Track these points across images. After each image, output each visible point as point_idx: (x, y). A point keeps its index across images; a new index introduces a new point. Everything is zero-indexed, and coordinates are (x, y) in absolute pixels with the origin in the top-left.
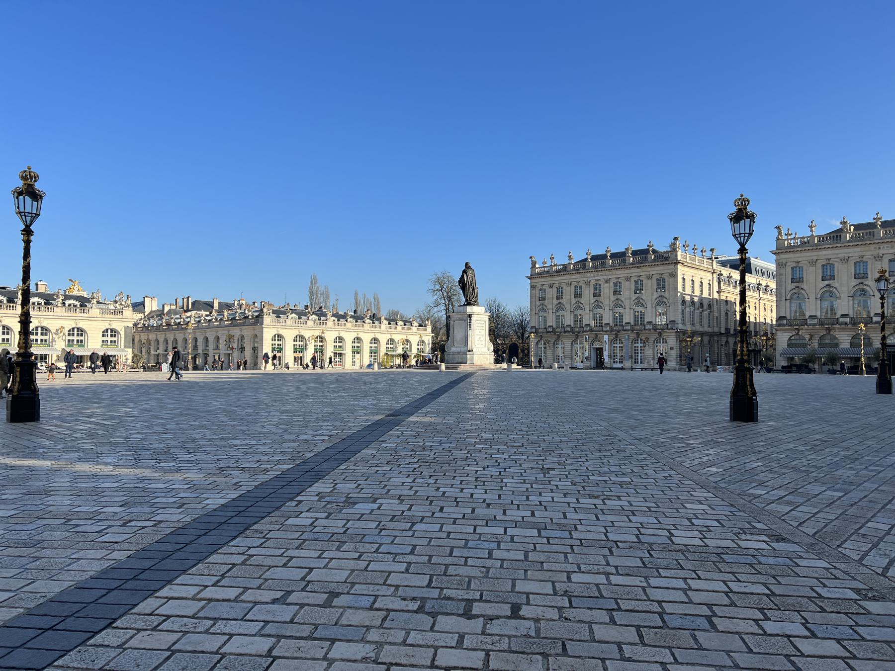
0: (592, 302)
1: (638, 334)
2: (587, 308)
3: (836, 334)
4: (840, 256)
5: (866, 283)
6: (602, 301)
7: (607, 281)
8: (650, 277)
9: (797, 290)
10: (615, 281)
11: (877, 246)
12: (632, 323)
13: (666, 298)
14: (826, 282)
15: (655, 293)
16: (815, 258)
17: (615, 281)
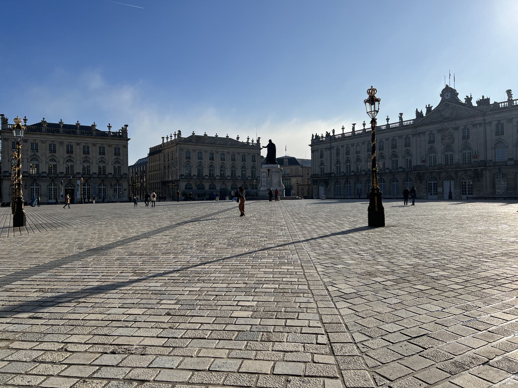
0: (66, 156)
1: (103, 181)
2: (61, 161)
3: (204, 183)
4: (205, 149)
5: (213, 162)
6: (74, 157)
7: (78, 144)
8: (110, 146)
9: (188, 163)
10: (100, 146)
11: (217, 147)
12: (47, 172)
13: (121, 160)
14: (200, 160)
15: (114, 156)
16: (195, 149)
17: (50, 143)
